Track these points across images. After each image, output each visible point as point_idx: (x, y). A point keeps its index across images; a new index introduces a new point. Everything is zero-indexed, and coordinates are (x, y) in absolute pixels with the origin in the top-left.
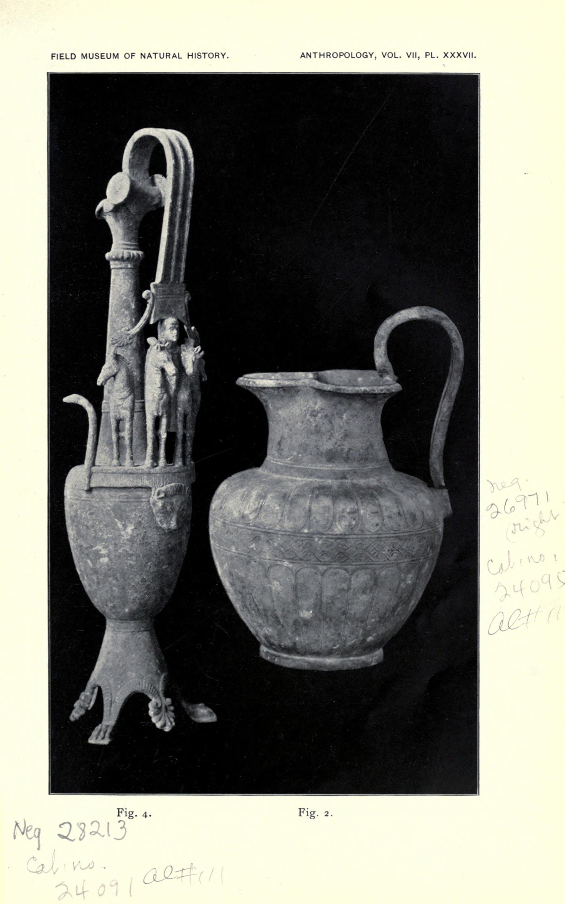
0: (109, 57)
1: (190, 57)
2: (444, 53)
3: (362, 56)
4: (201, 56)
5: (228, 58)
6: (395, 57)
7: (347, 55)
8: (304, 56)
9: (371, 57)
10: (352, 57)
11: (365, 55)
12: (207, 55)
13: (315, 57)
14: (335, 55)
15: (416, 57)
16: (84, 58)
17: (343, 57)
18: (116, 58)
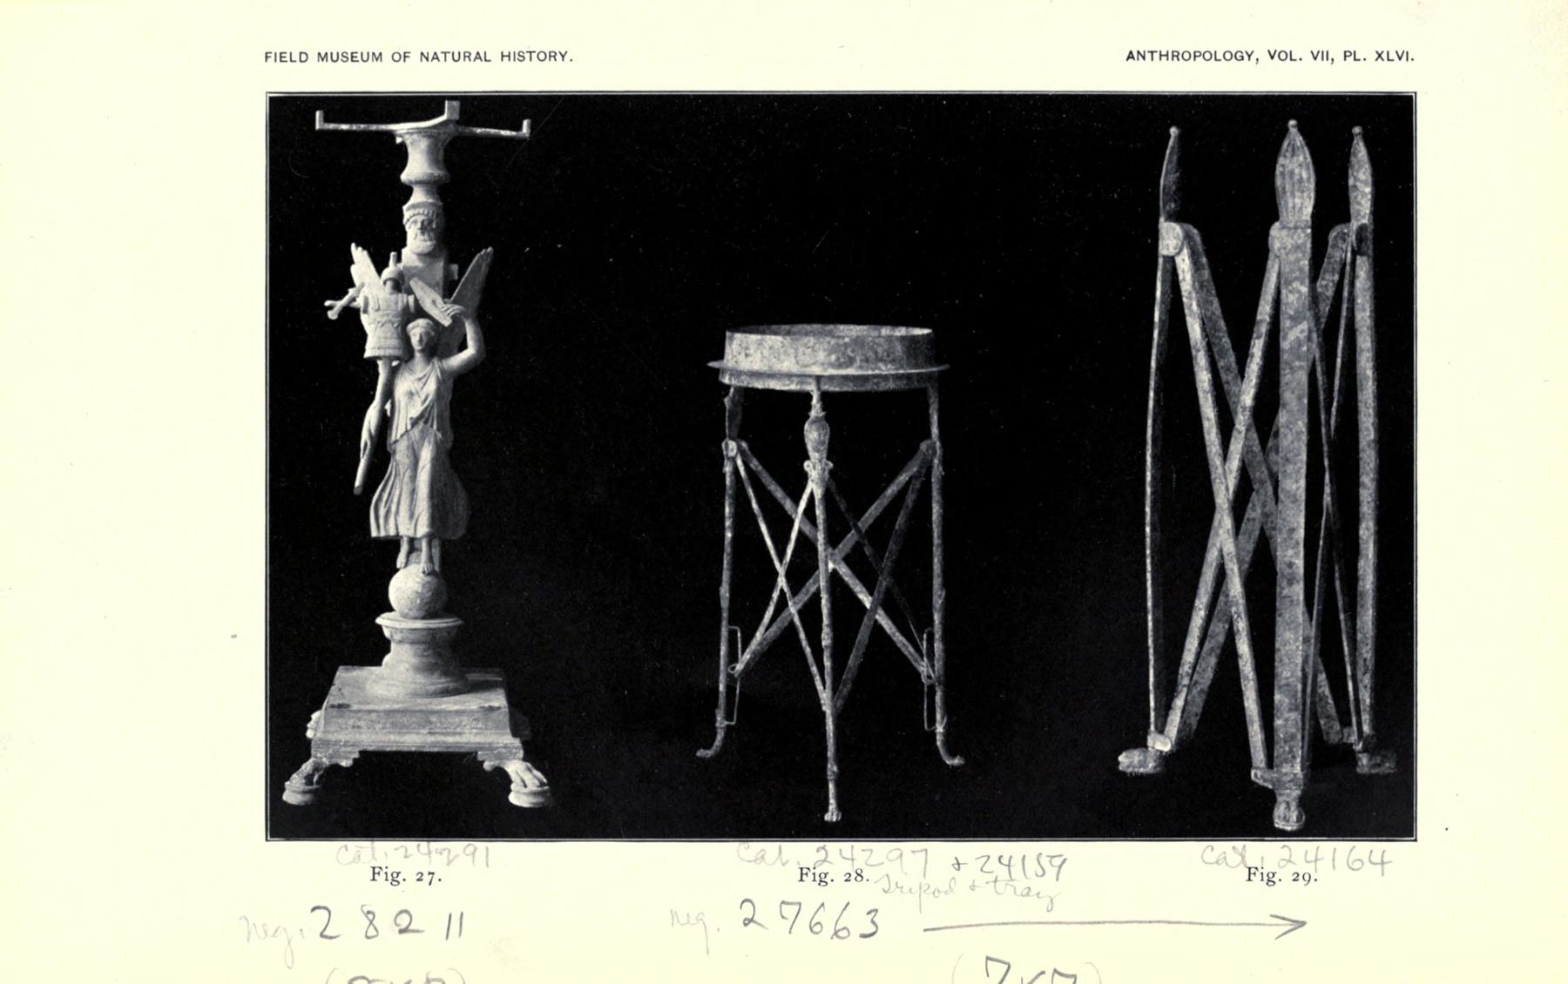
0: (365, 58)
1: (506, 59)
12: (534, 56)
16: (323, 60)
18: (377, 60)
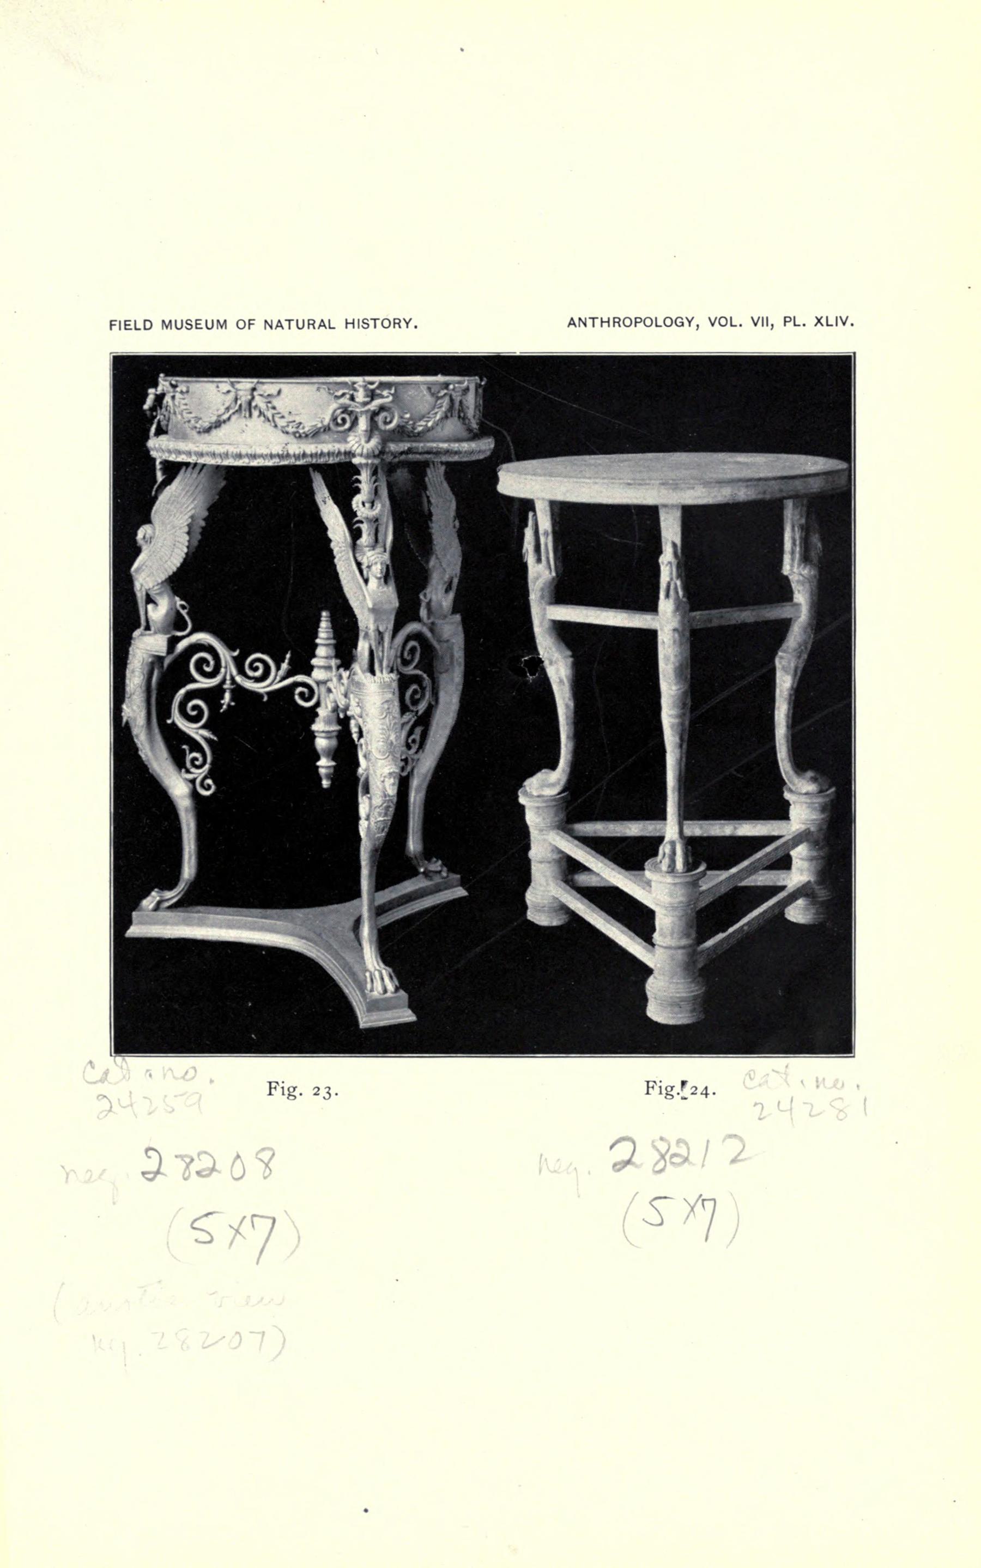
0: (210, 326)
1: (350, 326)
2: (816, 318)
3: (674, 324)
4: (368, 324)
5: (416, 327)
6: (731, 325)
7: (648, 322)
8: (574, 324)
9: (690, 326)
10: (657, 326)
11: (677, 322)
12: (378, 323)
13: (594, 326)
14: (627, 322)
15: (767, 325)
16: (167, 327)
17: (641, 325)
18: (222, 327)
